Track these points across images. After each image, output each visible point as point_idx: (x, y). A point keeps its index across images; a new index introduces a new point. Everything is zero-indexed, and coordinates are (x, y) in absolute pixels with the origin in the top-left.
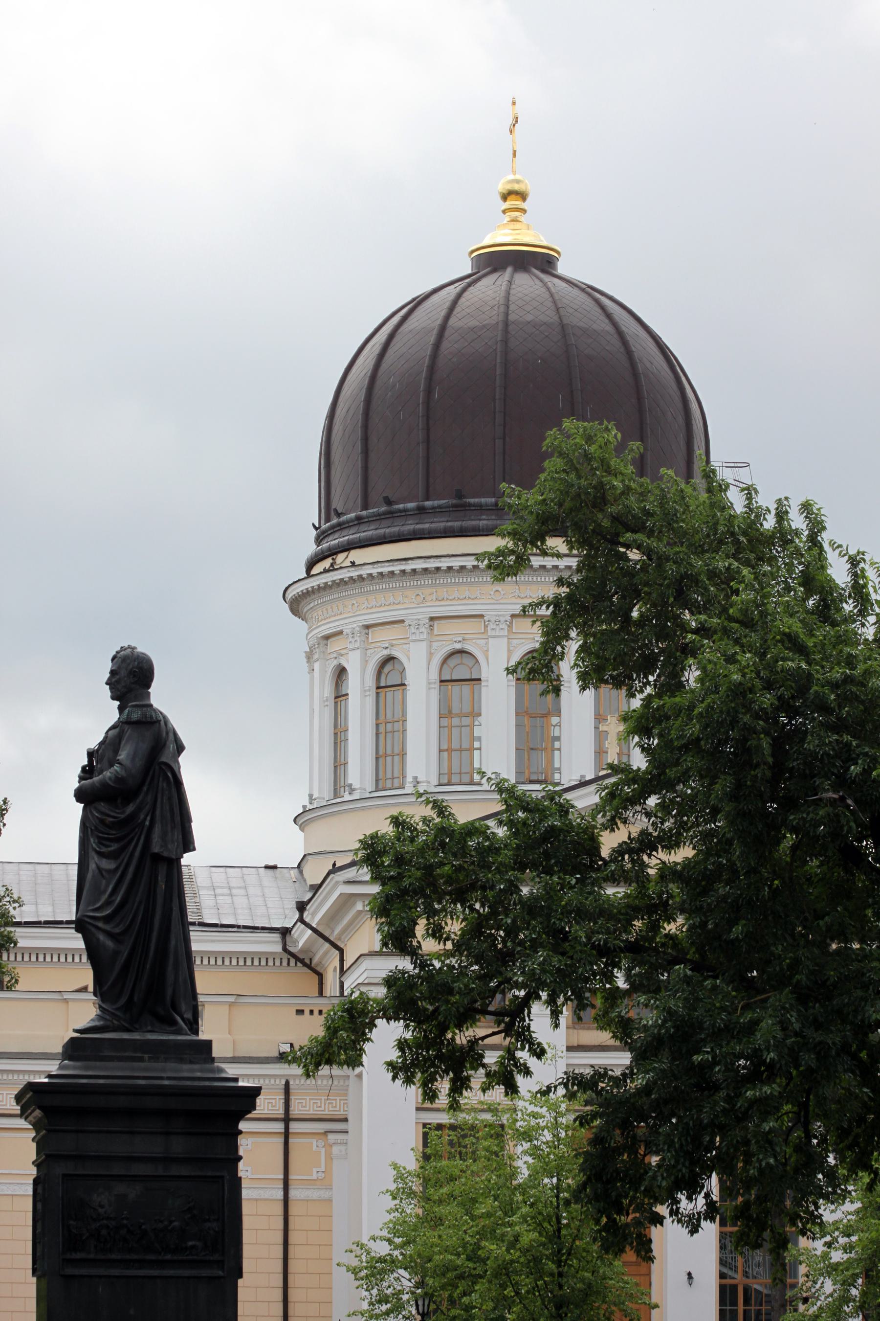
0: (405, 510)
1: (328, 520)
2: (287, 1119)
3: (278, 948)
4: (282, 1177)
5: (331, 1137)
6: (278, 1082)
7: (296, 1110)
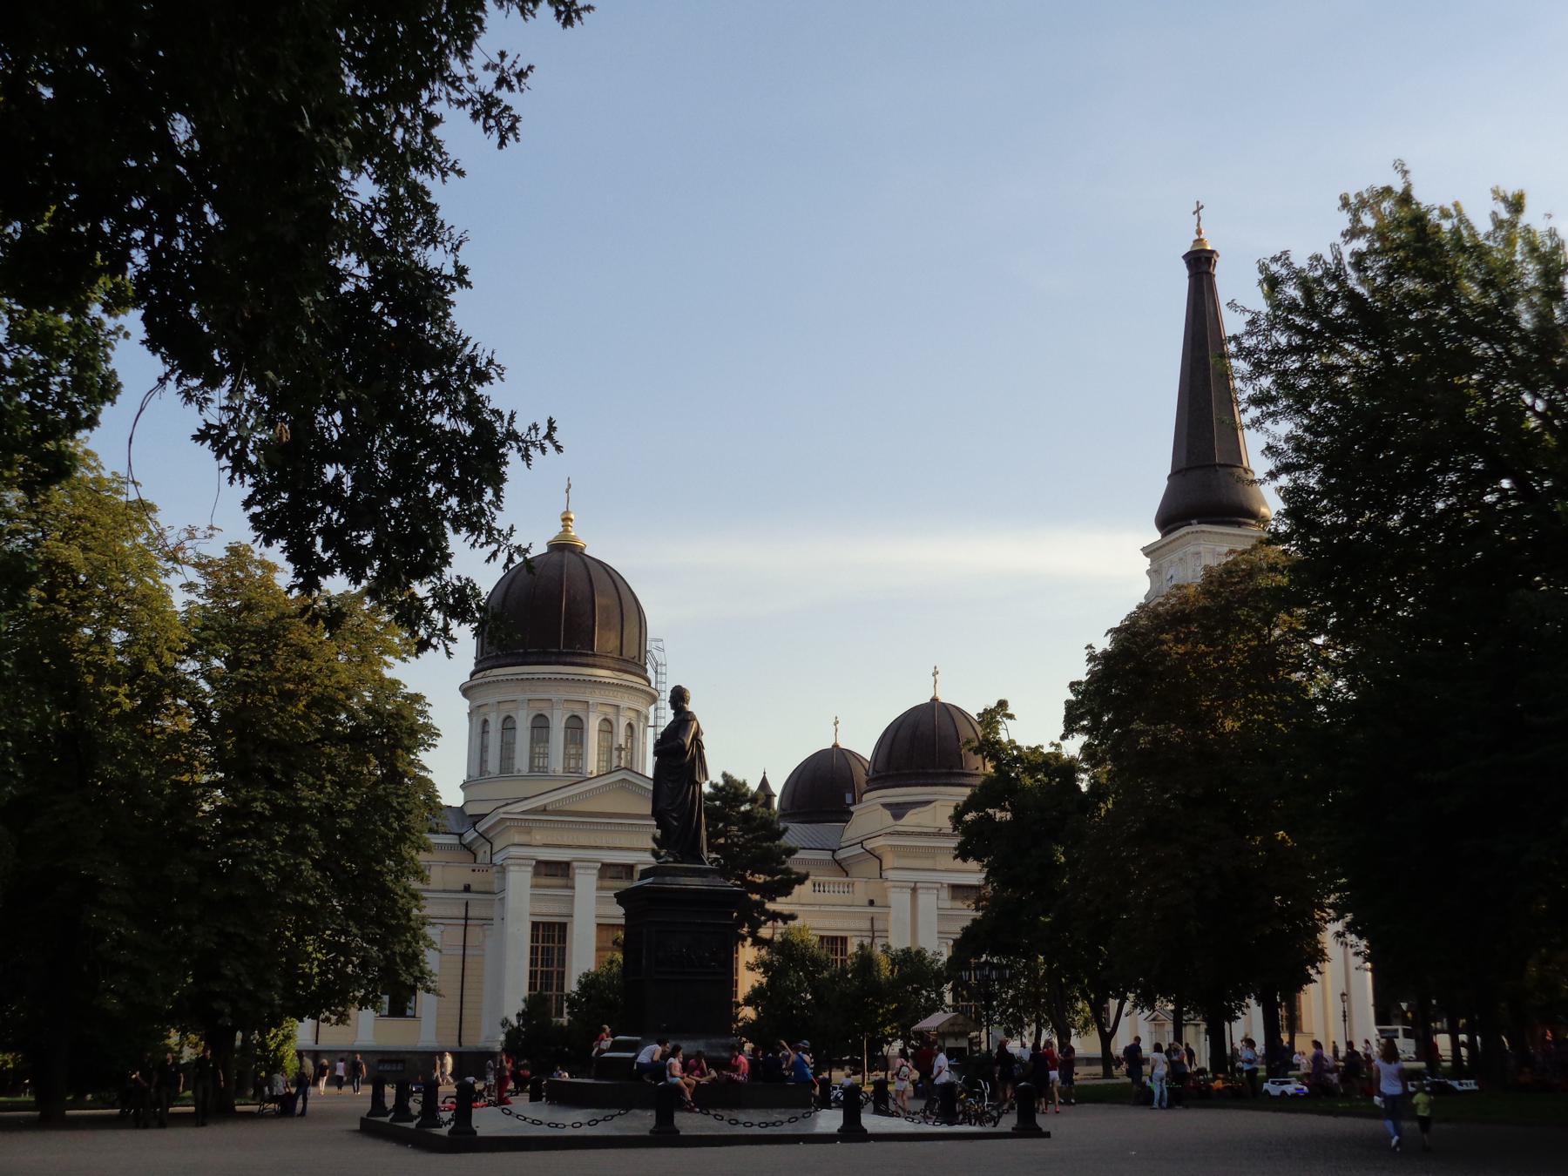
1: (482, 655)
2: (466, 918)
3: (458, 842)
7: (470, 914)
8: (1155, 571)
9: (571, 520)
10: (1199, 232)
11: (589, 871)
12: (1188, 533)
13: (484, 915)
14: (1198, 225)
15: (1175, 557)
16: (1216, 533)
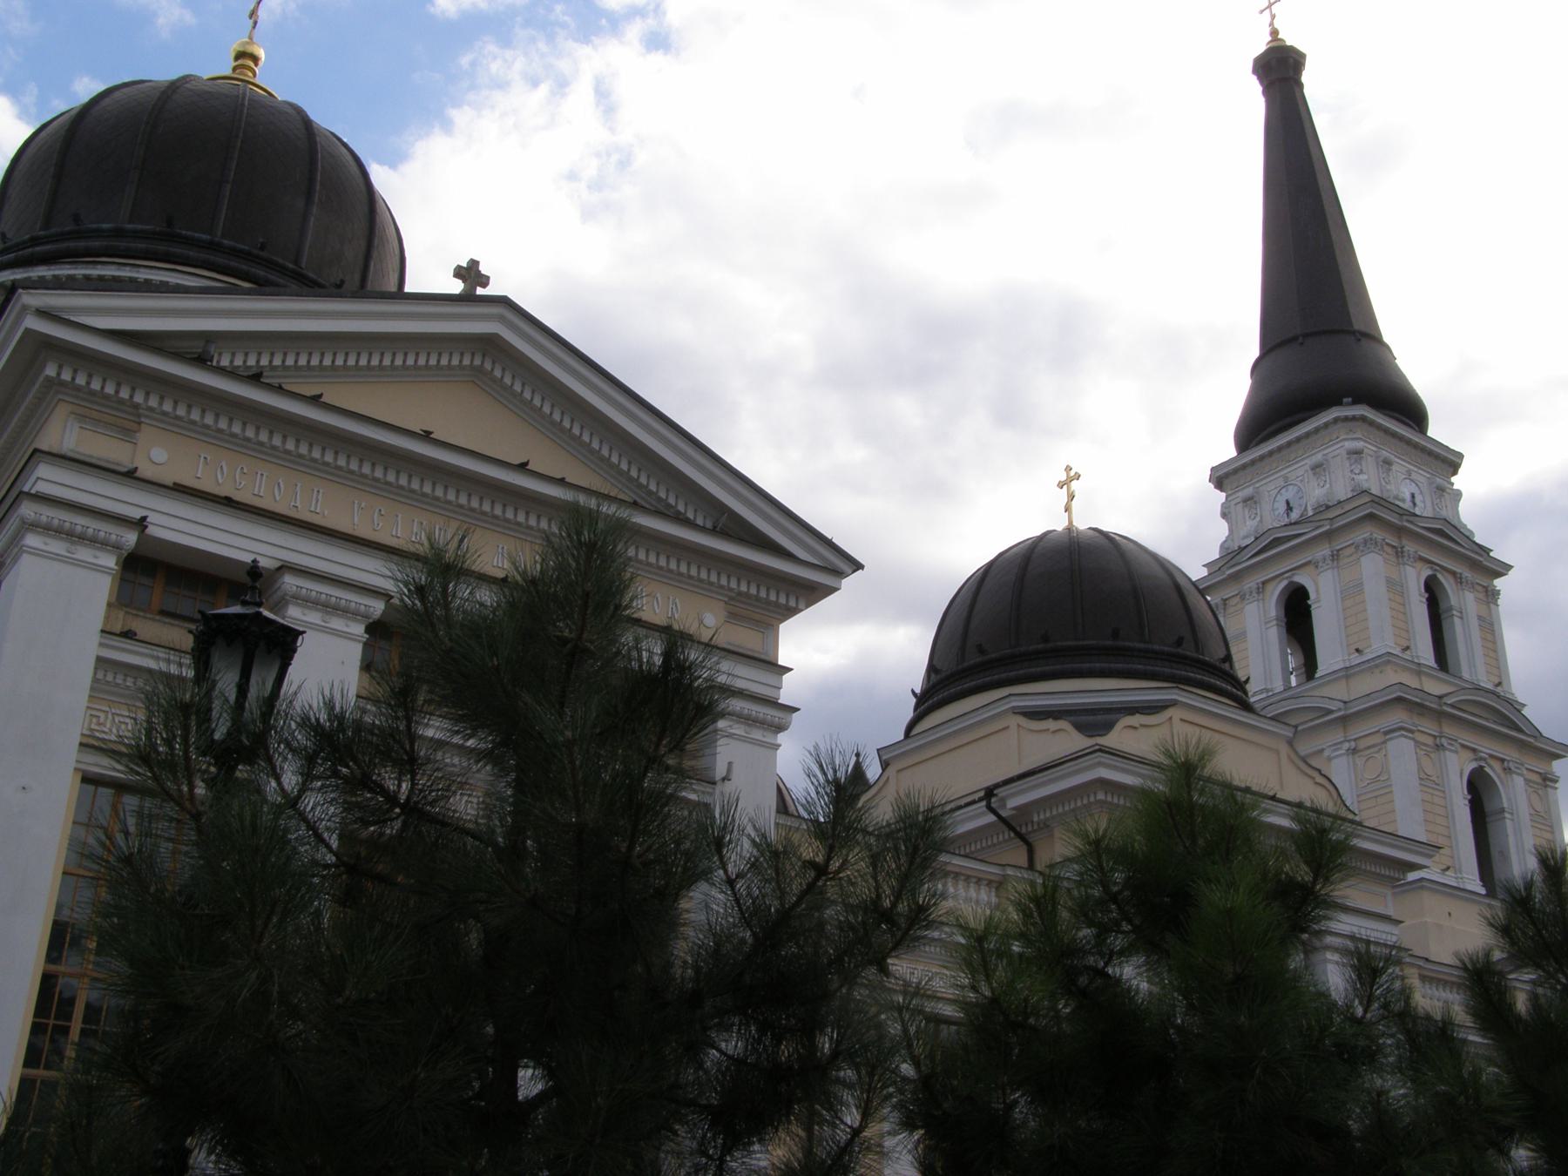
8: (1246, 500)
9: (255, 59)
10: (1274, 33)
12: (1336, 420)
14: (1271, 24)
15: (1300, 469)
16: (1379, 427)
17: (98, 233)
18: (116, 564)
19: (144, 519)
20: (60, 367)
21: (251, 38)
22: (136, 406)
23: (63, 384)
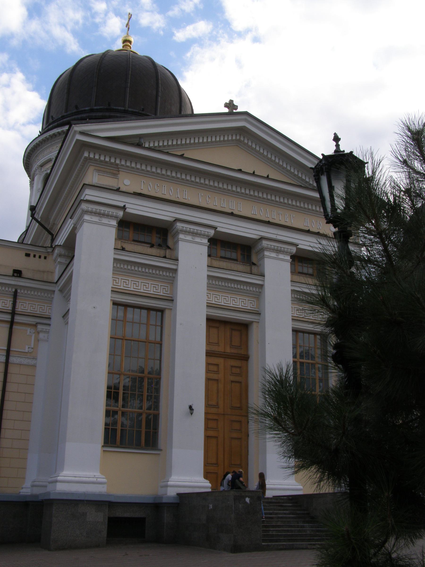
0: (85, 110)
2: (13, 313)
4: (6, 348)
5: (40, 327)
6: (10, 289)
7: (19, 308)
9: (130, 42)
11: (198, 240)
13: (38, 311)
17: (84, 112)
18: (116, 224)
19: (125, 206)
20: (89, 153)
21: (128, 34)
22: (117, 165)
23: (91, 159)
